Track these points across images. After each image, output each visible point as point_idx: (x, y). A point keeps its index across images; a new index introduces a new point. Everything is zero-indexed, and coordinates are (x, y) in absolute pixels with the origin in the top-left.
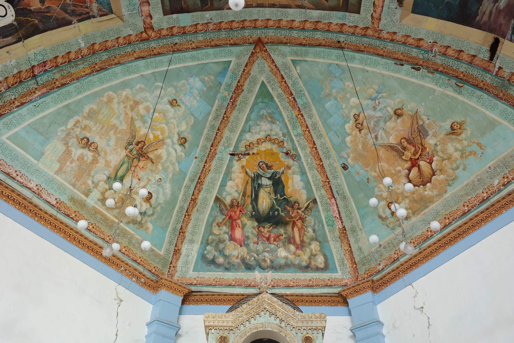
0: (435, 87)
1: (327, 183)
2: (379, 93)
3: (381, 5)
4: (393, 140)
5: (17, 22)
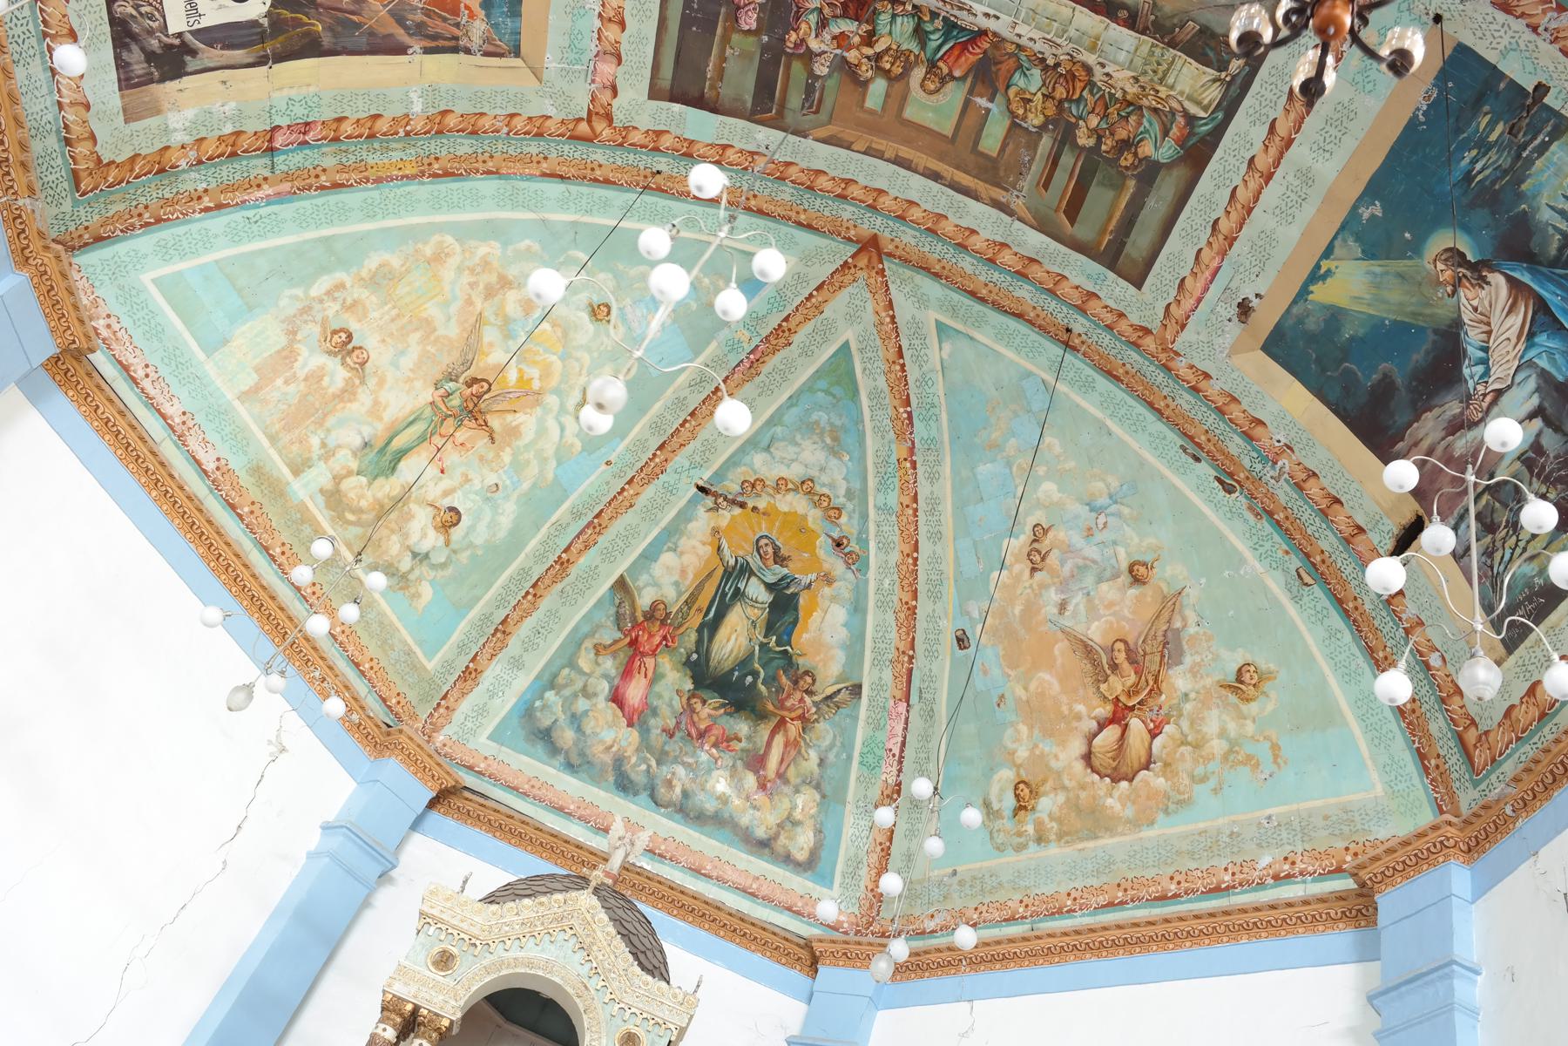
0: (1248, 554)
1: (906, 659)
2: (1116, 502)
3: (1197, 293)
4: (1096, 633)
5: (270, 21)
